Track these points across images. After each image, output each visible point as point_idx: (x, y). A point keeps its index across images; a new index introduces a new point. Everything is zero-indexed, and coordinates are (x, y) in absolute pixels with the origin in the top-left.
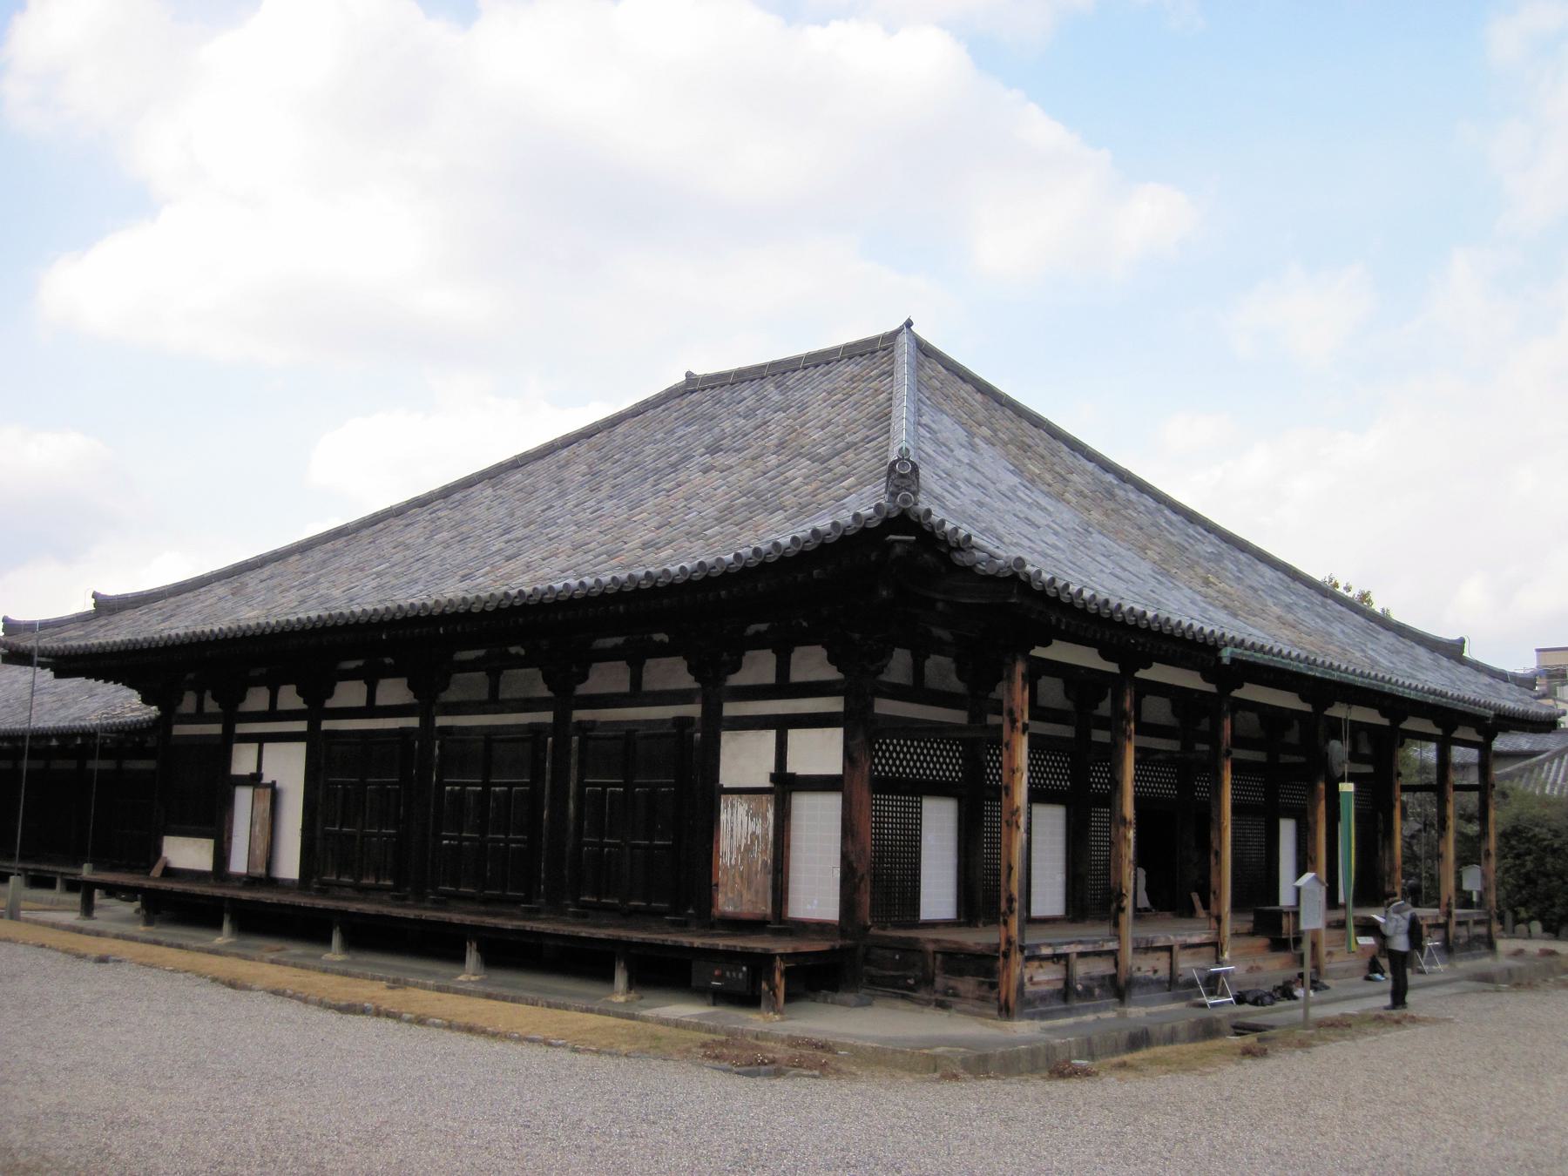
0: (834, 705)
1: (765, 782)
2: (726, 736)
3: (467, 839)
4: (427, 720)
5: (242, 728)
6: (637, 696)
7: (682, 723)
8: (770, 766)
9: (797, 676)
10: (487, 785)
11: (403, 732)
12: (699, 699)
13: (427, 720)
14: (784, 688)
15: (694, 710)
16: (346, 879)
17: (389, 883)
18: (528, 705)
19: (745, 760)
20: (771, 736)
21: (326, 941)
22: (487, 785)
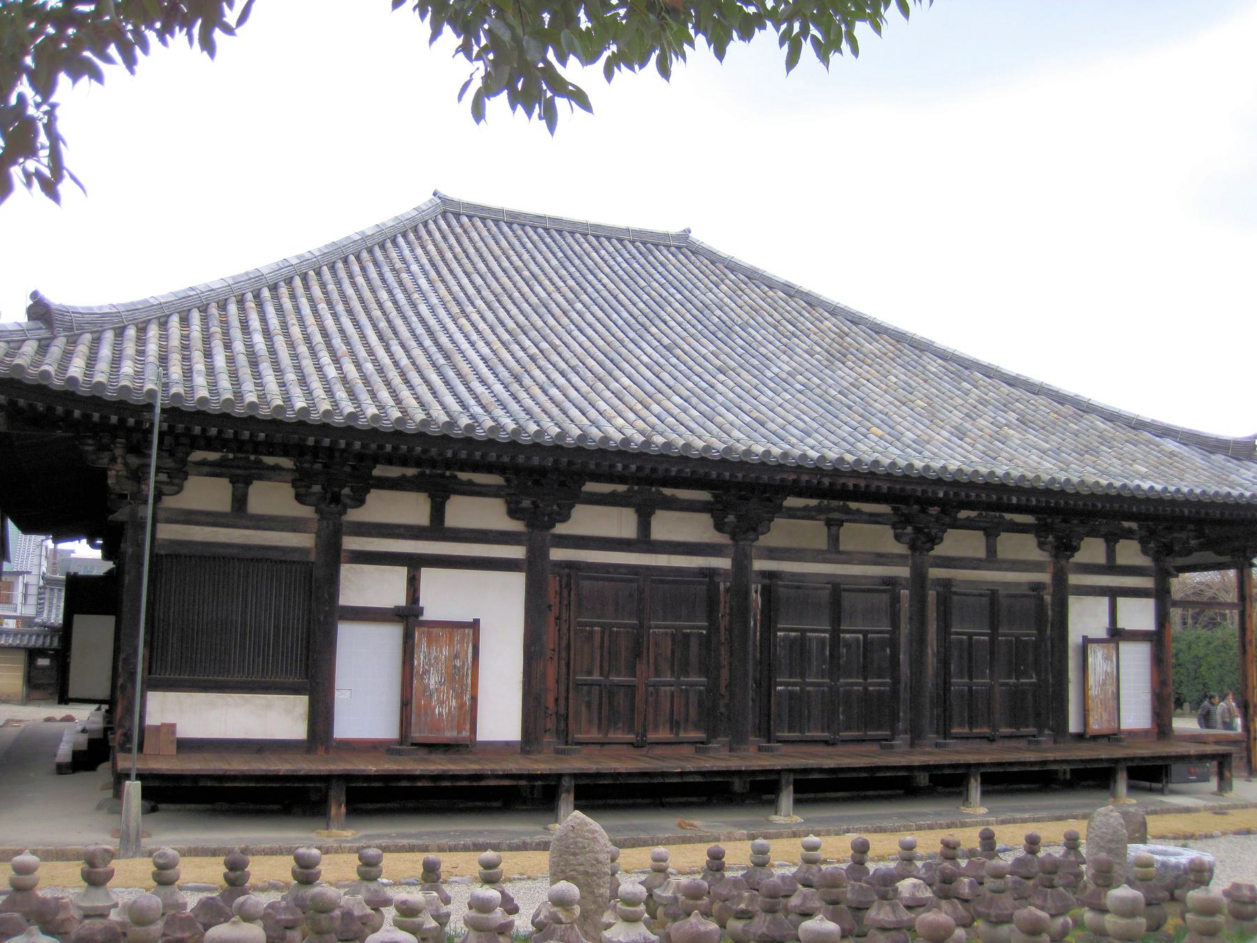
0: (1147, 582)
1: (1103, 634)
2: (1072, 600)
3: (812, 684)
4: (741, 564)
5: (352, 543)
6: (991, 560)
7: (1037, 587)
8: (1105, 621)
9: (1121, 560)
10: (836, 633)
11: (709, 573)
12: (1050, 569)
13: (741, 564)
14: (1111, 568)
15: (1045, 577)
16: (614, 735)
17: (701, 735)
18: (879, 558)
19: (1086, 618)
20: (1105, 601)
21: (773, 804)
22: (836, 633)
